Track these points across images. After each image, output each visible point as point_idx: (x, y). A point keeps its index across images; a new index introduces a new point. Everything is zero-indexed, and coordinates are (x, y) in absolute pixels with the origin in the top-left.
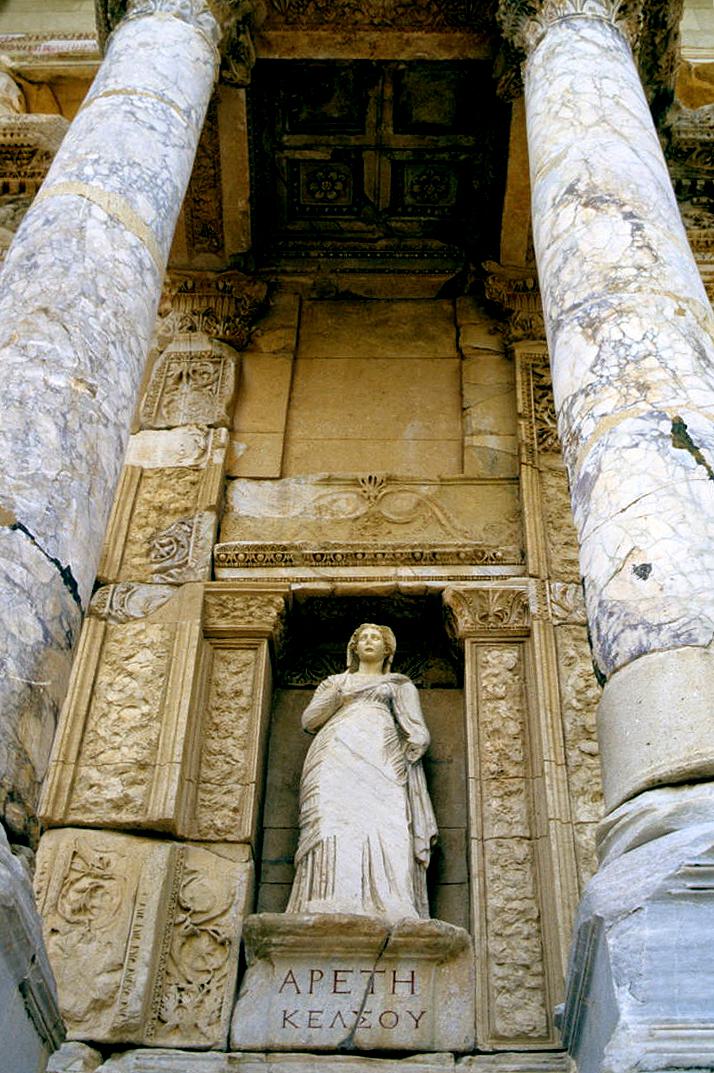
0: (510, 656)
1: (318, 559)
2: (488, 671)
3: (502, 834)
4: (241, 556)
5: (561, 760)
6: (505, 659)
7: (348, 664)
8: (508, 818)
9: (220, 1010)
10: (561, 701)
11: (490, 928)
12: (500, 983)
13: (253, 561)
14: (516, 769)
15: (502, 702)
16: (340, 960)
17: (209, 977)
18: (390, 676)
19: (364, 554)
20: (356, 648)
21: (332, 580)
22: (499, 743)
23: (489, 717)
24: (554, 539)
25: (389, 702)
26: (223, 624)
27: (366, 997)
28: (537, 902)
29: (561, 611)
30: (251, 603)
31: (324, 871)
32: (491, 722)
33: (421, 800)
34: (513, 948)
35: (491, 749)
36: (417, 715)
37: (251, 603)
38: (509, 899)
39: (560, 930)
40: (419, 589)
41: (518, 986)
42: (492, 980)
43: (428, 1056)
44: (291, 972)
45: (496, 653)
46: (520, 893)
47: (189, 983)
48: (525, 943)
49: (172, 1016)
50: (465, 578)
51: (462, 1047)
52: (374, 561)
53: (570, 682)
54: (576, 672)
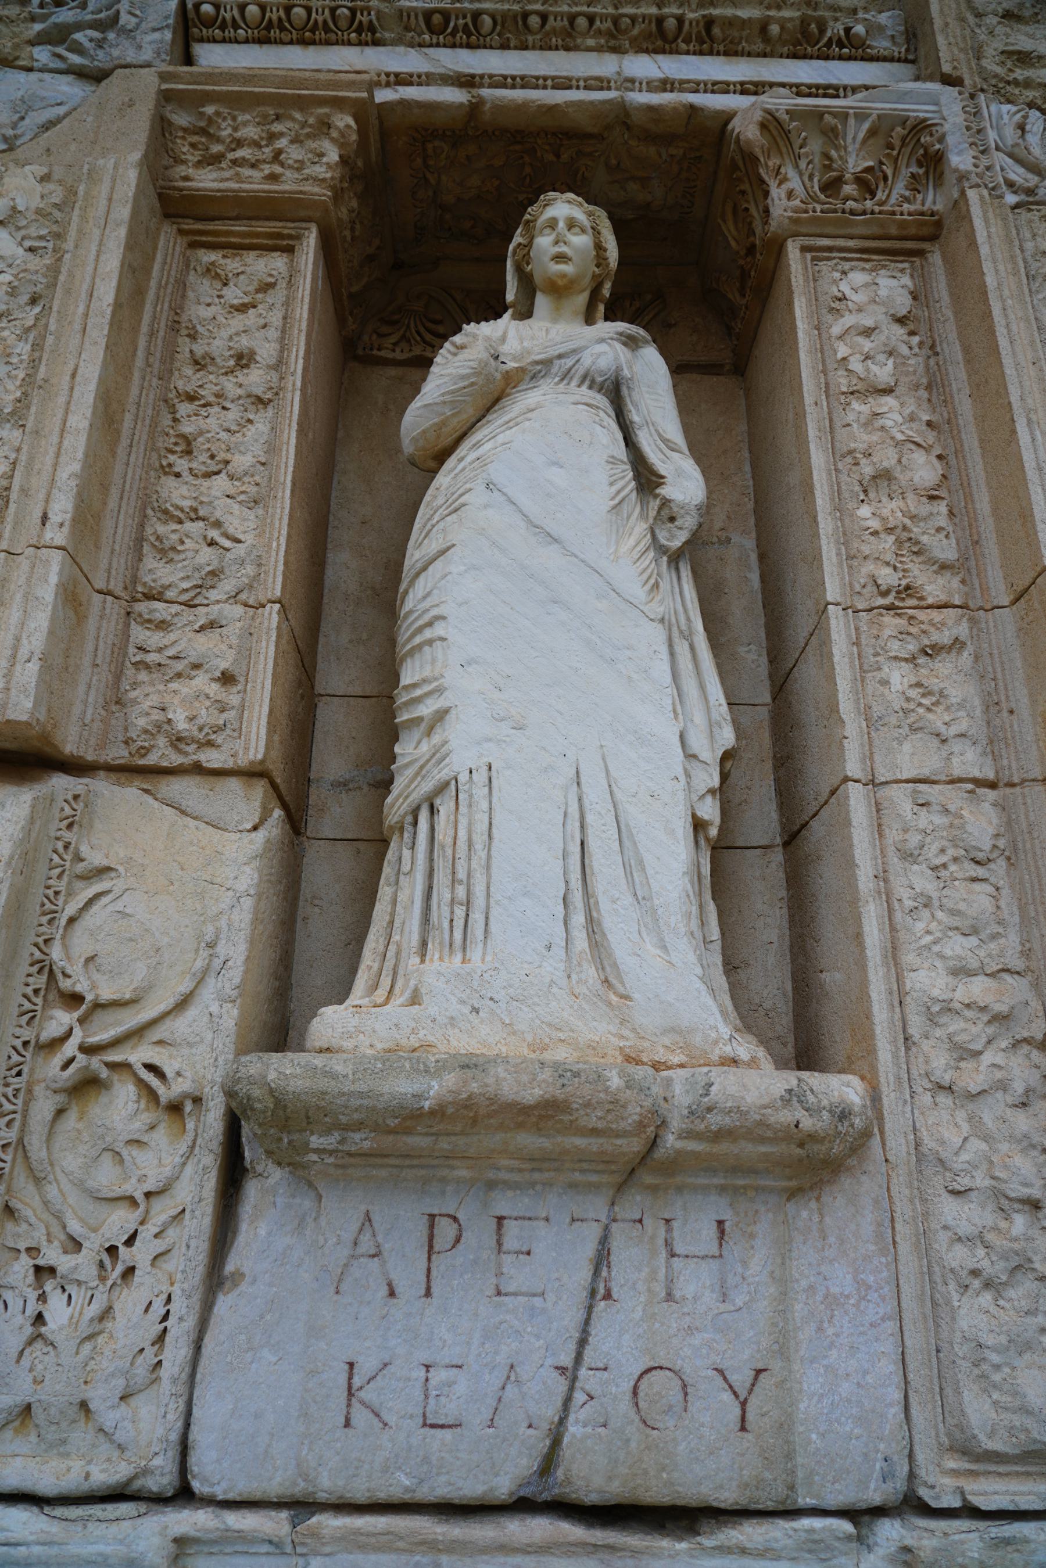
0: (893, 286)
2: (849, 320)
3: (925, 772)
6: (883, 292)
7: (510, 297)
8: (937, 720)
14: (941, 581)
15: (889, 401)
18: (606, 328)
19: (544, 17)
20: (527, 258)
21: (467, 81)
22: (892, 509)
23: (862, 439)
25: (615, 392)
26: (207, 180)
27: (590, 1309)
30: (277, 127)
33: (692, 648)
34: (986, 1138)
35: (875, 524)
36: (672, 428)
37: (277, 127)
38: (960, 971)
41: (1018, 1267)
43: (777, 1531)
45: (858, 277)
48: (1022, 1122)
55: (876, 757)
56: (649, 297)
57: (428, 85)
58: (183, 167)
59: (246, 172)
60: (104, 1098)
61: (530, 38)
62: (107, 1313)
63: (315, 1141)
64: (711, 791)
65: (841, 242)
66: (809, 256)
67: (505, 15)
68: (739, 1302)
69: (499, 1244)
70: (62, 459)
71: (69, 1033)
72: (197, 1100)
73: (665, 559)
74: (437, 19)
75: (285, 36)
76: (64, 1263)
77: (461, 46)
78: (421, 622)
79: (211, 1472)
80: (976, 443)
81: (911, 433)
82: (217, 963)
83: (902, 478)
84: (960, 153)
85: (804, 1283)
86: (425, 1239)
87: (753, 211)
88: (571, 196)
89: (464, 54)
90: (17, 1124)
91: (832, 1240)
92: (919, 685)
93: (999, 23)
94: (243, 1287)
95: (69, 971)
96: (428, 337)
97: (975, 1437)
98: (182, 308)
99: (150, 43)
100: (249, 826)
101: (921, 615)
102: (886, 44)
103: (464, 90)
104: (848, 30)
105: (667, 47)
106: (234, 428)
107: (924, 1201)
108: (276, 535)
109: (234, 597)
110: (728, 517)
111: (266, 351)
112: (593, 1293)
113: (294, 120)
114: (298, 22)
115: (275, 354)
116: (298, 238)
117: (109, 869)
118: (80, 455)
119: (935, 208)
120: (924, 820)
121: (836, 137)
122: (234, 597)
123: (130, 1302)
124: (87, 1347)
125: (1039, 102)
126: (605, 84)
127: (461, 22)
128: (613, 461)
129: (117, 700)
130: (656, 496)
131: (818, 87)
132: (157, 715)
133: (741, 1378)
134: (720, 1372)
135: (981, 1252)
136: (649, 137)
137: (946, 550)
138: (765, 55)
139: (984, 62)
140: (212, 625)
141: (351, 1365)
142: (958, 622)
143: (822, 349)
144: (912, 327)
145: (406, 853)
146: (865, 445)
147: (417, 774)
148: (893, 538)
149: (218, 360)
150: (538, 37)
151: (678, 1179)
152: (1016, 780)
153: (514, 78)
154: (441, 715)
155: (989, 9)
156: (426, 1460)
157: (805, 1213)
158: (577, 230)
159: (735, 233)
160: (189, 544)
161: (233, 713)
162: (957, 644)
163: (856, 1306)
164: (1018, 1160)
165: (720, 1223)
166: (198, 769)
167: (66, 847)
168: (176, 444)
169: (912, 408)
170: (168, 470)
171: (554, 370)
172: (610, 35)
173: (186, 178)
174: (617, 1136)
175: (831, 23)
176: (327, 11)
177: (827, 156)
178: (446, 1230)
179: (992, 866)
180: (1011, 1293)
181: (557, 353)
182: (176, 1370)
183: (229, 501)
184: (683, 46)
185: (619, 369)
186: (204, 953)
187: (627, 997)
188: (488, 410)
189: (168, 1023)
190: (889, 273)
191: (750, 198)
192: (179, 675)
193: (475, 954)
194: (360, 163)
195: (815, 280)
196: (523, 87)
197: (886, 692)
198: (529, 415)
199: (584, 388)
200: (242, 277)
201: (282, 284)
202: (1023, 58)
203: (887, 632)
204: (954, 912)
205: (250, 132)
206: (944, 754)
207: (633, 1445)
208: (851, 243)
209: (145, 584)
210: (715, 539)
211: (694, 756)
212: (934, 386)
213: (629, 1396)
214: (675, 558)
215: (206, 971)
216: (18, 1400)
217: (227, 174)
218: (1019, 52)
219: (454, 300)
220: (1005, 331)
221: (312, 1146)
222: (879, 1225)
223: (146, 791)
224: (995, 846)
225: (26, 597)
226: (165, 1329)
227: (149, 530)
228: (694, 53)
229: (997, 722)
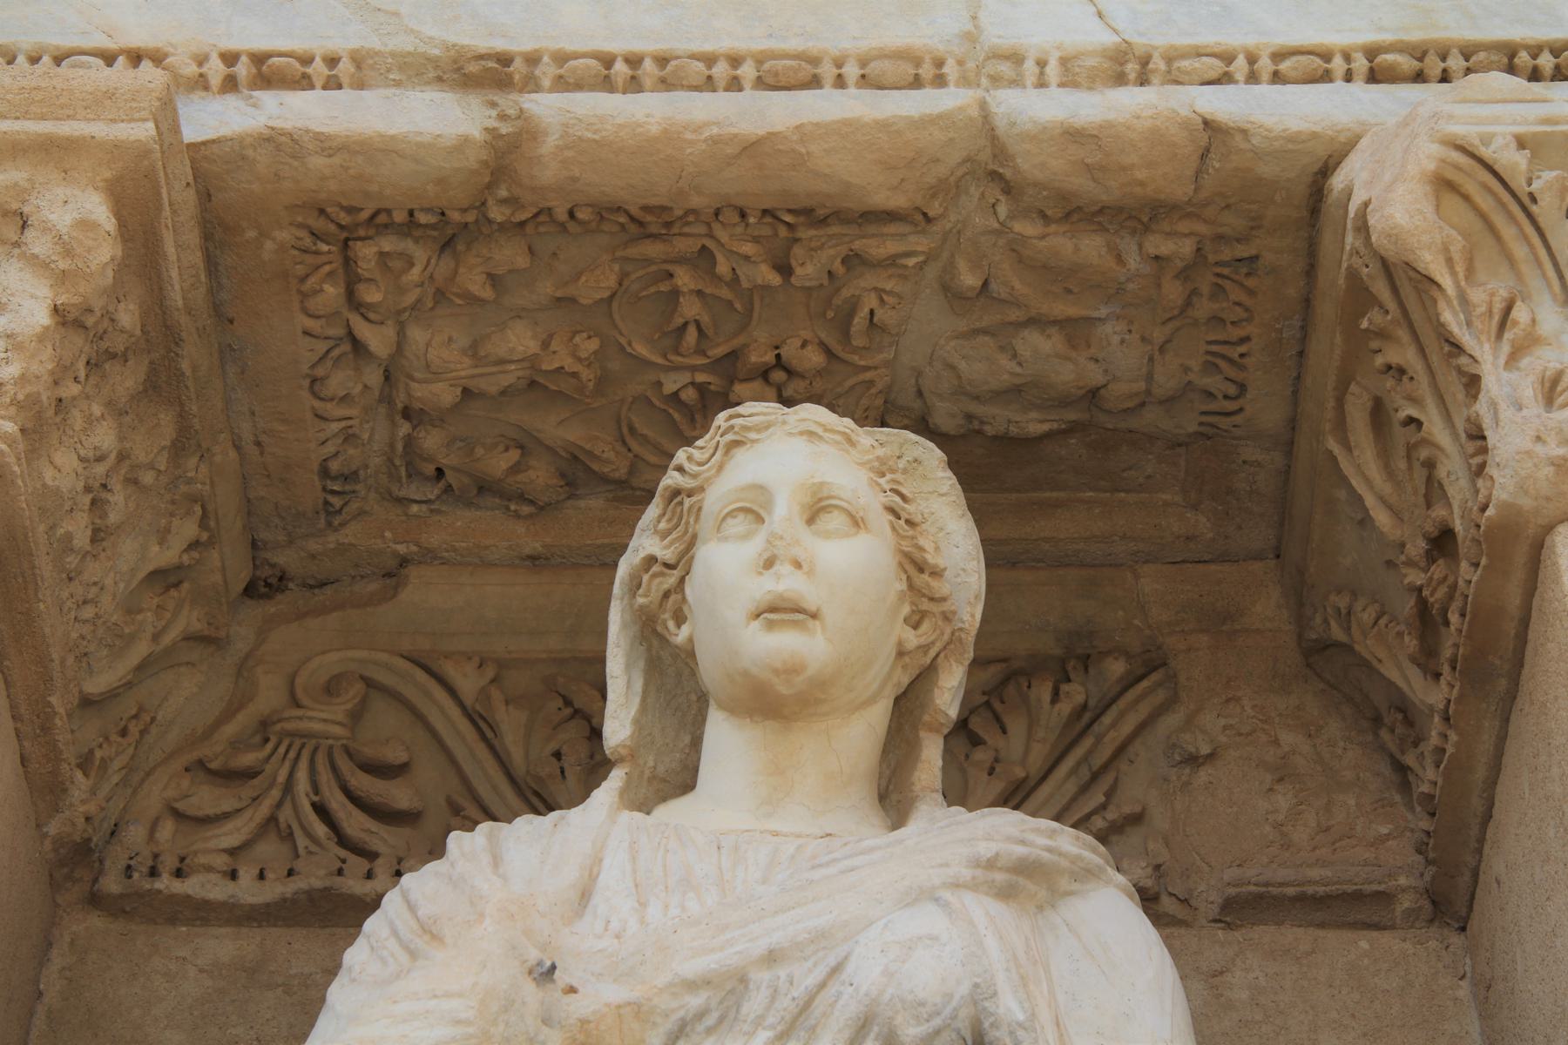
7: (617, 728)
20: (675, 602)
56: (1116, 668)
57: (360, 85)
87: (1436, 428)
96: (355, 823)
126: (927, 71)
136: (1074, 212)
153: (634, 61)
158: (835, 521)
159: (1387, 489)
171: (754, 1005)
181: (760, 947)
185: (981, 995)
191: (1423, 386)
194: (128, 316)
196: (666, 84)
219: (452, 691)
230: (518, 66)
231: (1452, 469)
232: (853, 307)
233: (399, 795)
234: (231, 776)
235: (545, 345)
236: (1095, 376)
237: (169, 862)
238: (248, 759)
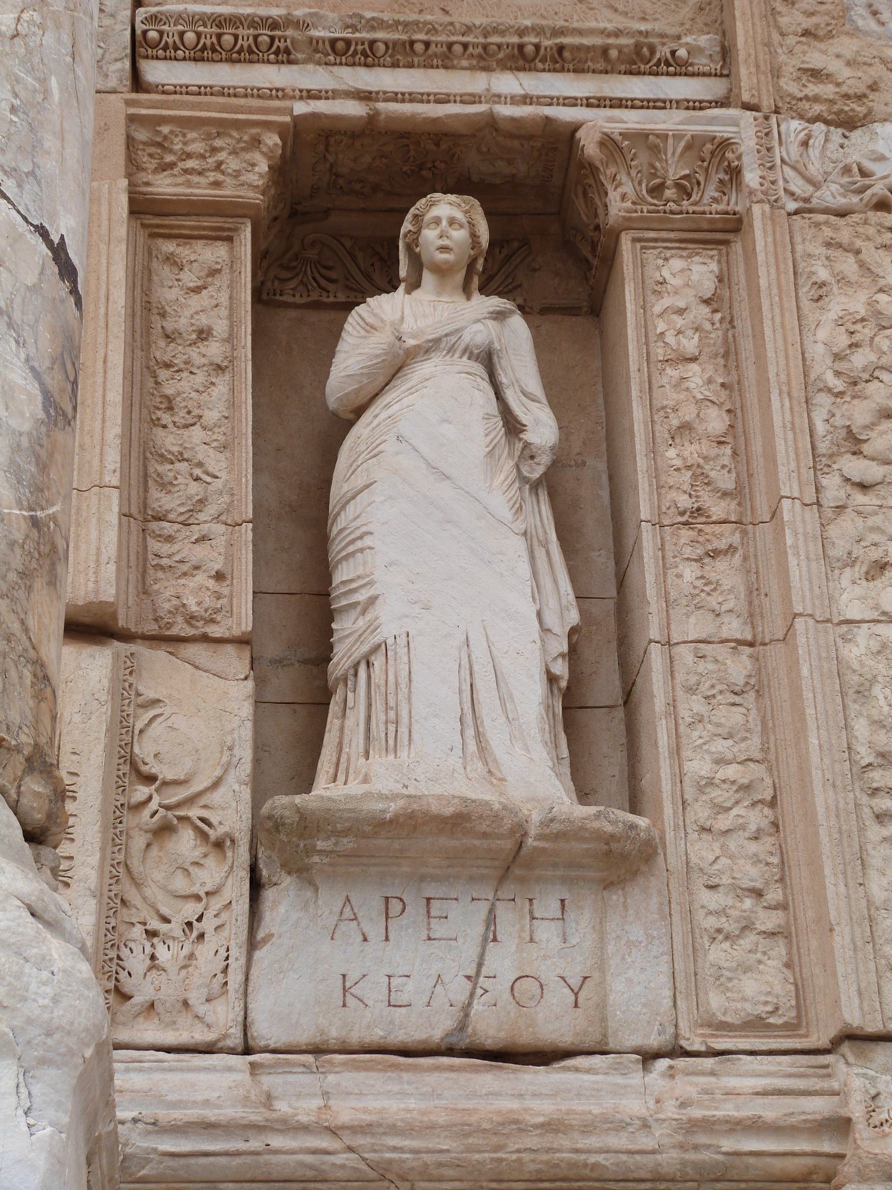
1: (341, 51)
2: (666, 302)
3: (704, 636)
4: (190, 36)
5: (810, 496)
6: (695, 277)
7: (403, 273)
8: (713, 601)
9: (225, 970)
10: (805, 376)
11: (690, 817)
12: (711, 922)
13: (214, 50)
14: (723, 504)
15: (695, 367)
16: (435, 879)
17: (199, 908)
22: (691, 451)
24: (783, 21)
25: (488, 360)
26: (164, 186)
28: (770, 770)
29: (801, 182)
30: (218, 143)
31: (392, 703)
32: (675, 410)
33: (548, 553)
34: (731, 857)
35: (678, 463)
36: (533, 384)
37: (218, 143)
38: (721, 761)
39: (822, 832)
40: (533, 120)
41: (744, 928)
42: (700, 915)
43: (597, 1060)
44: (348, 900)
45: (677, 264)
46: (740, 750)
47: (167, 920)
49: (143, 989)
50: (619, 103)
51: (654, 1041)
52: (445, 58)
53: (822, 334)
54: (832, 315)
55: (672, 627)
56: (516, 244)
57: (333, 98)
58: (143, 174)
59: (195, 179)
60: (174, 838)
61: (416, 60)
62: (191, 956)
63: (320, 845)
64: (562, 655)
65: (664, 235)
66: (638, 245)
67: (395, 43)
68: (574, 942)
69: (428, 912)
70: (108, 424)
71: (150, 798)
72: (233, 841)
73: (527, 486)
74: (340, 45)
75: (216, 56)
76: (163, 927)
77: (360, 65)
78: (353, 536)
79: (266, 1030)
80: (756, 400)
81: (707, 393)
82: (235, 760)
83: (700, 428)
84: (751, 171)
85: (614, 935)
86: (384, 910)
87: (597, 200)
88: (452, 197)
89: (362, 71)
90: (123, 851)
91: (631, 912)
92: (702, 577)
93: (798, 43)
94: (274, 940)
95: (146, 760)
96: (323, 283)
97: (714, 1014)
98: (150, 290)
99: (114, 72)
100: (243, 677)
101: (708, 529)
102: (705, 61)
103: (363, 103)
104: (673, 53)
105: (527, 66)
106: (201, 389)
107: (690, 894)
108: (244, 473)
109: (217, 518)
110: (584, 444)
111: (220, 327)
112: (485, 940)
113: (231, 136)
114: (227, 46)
115: (226, 328)
116: (236, 230)
117: (159, 701)
118: (119, 422)
119: (737, 209)
120: (702, 666)
121: (660, 152)
122: (217, 518)
123: (205, 951)
124: (183, 973)
125: (825, 115)
126: (477, 99)
127: (360, 48)
128: (487, 417)
129: (145, 591)
130: (520, 439)
131: (649, 101)
132: (175, 602)
133: (575, 982)
134: (563, 978)
135: (724, 919)
136: (512, 136)
137: (727, 482)
138: (607, 72)
139: (782, 82)
140: (203, 539)
141: (344, 976)
142: (733, 533)
143: (645, 326)
144: (715, 306)
145: (350, 695)
146: (674, 403)
147: (357, 641)
148: (690, 473)
149: (184, 335)
150: (422, 59)
151: (538, 872)
152: (767, 641)
153: (403, 94)
154: (372, 600)
155: (790, 30)
156: (392, 1022)
157: (615, 897)
158: (456, 226)
160: (181, 480)
161: (226, 600)
162: (731, 550)
163: (646, 947)
164: (748, 867)
165: (562, 901)
166: (205, 638)
167: (131, 685)
168: (161, 402)
169: (711, 373)
170: (156, 423)
171: (443, 345)
172: (480, 57)
173: (148, 184)
174: (499, 839)
175: (659, 48)
176: (251, 39)
177: (652, 166)
178: (395, 906)
179: (745, 695)
180: (742, 942)
182: (237, 986)
183: (206, 447)
184: (540, 66)
185: (491, 343)
186: (227, 753)
187: (502, 780)
188: (393, 376)
189: (208, 794)
190: (701, 260)
192: (185, 574)
193: (403, 753)
195: (643, 266)
196: (411, 101)
197: (680, 582)
198: (425, 383)
199: (465, 359)
200: (195, 264)
201: (226, 270)
202: (815, 74)
203: (683, 541)
204: (718, 725)
205: (197, 147)
206: (718, 624)
207: (512, 1014)
208: (672, 235)
209: (153, 509)
210: (573, 463)
211: (549, 630)
212: (729, 353)
213: (509, 990)
214: (535, 486)
215: (229, 763)
216: (147, 998)
217: (180, 180)
218: (813, 70)
220: (770, 323)
221: (318, 848)
222: (661, 904)
223: (171, 653)
224: (747, 683)
225: (99, 519)
226: (227, 966)
227: (151, 470)
228: (549, 71)
229: (756, 602)
230: (373, 95)
231: (601, 211)
232: (454, 154)
233: (333, 275)
234: (288, 268)
235: (374, 159)
236: (514, 171)
237: (278, 292)
238: (294, 264)
